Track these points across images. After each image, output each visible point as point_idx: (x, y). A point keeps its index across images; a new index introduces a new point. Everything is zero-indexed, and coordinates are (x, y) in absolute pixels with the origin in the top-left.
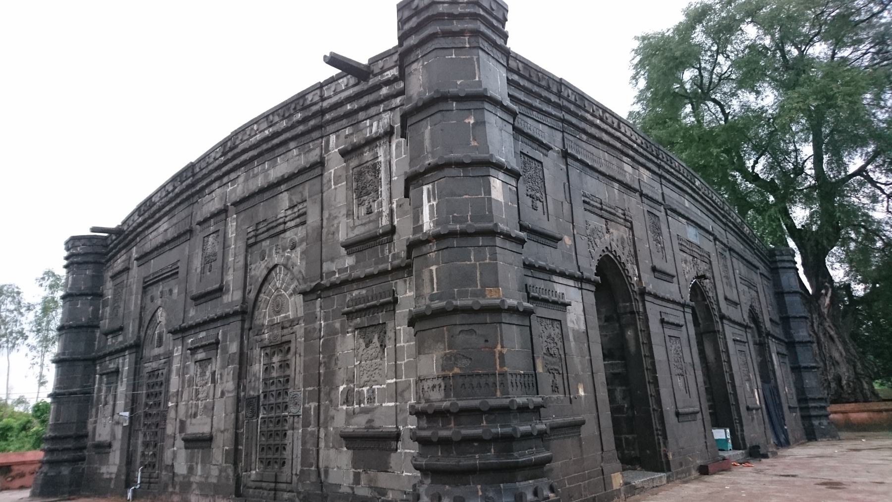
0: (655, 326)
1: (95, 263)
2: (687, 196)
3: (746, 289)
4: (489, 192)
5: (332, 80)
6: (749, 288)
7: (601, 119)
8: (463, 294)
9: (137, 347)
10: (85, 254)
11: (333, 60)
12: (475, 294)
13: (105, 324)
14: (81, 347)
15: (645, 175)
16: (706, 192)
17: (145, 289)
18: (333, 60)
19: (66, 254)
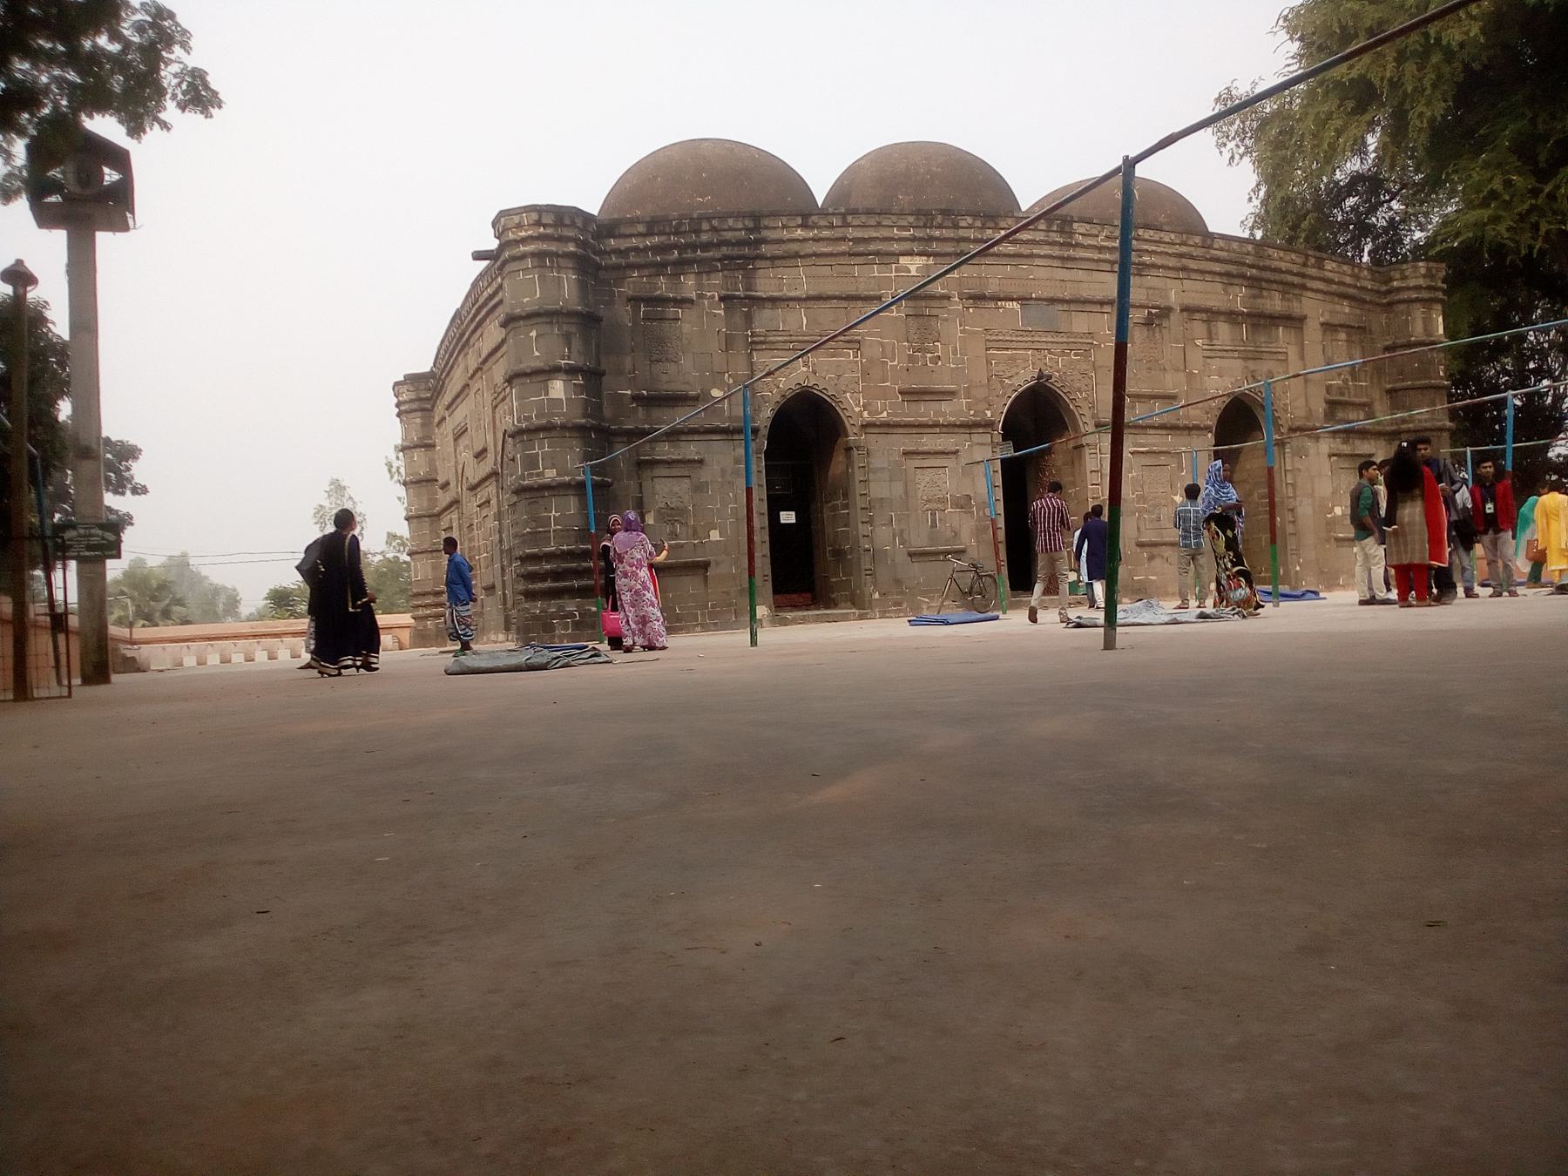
0: (877, 462)
1: (422, 410)
3: (1238, 364)
4: (547, 394)
5: (487, 269)
6: (1245, 359)
7: (804, 226)
8: (531, 475)
9: (455, 502)
10: (411, 401)
11: (478, 256)
12: (538, 475)
13: (441, 480)
14: (425, 504)
15: (914, 265)
17: (457, 438)
18: (478, 256)
19: (395, 400)
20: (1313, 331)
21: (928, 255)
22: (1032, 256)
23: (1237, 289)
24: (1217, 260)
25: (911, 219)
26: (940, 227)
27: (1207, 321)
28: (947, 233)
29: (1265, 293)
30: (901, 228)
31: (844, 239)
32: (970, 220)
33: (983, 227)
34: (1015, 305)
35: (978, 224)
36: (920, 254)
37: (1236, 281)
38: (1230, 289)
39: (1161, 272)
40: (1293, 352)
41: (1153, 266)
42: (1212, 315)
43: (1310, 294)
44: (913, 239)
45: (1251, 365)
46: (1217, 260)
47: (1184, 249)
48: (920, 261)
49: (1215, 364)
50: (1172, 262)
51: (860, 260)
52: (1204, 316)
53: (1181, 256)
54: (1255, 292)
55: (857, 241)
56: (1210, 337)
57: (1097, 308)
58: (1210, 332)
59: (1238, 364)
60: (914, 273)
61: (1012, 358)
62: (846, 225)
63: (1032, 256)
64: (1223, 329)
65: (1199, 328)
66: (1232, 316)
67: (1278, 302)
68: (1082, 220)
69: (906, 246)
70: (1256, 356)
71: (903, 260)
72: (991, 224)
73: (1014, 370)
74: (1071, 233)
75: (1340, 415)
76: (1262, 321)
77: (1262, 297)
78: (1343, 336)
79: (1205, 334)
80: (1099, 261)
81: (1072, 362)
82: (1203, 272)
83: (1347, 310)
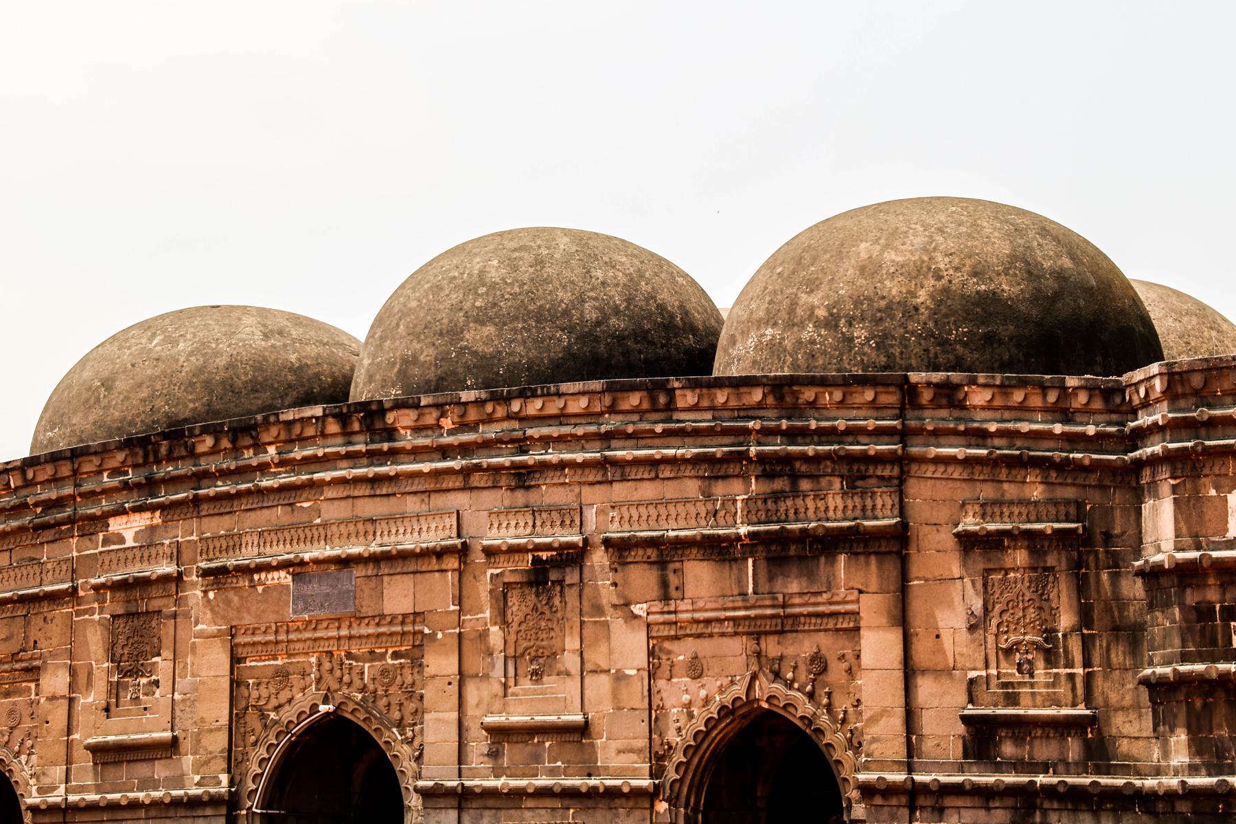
2: (330, 493)
6: (757, 636)
15: (129, 528)
16: (473, 415)
20: (936, 555)
21: (152, 508)
22: (314, 486)
23: (736, 486)
24: (682, 433)
25: (120, 456)
26: (170, 458)
27: (662, 564)
28: (185, 468)
29: (805, 485)
30: (115, 472)
31: (22, 507)
32: (209, 441)
33: (236, 451)
34: (284, 578)
35: (225, 443)
36: (138, 509)
37: (733, 469)
38: (720, 489)
39: (568, 476)
40: (873, 608)
41: (544, 466)
42: (665, 554)
43: (929, 470)
44: (126, 486)
45: (772, 647)
46: (682, 433)
47: (611, 423)
48: (141, 521)
49: (682, 652)
50: (591, 454)
51: (48, 535)
52: (652, 553)
53: (607, 437)
54: (779, 484)
55: (49, 505)
56: (665, 597)
57: (434, 563)
58: (664, 584)
59: (736, 649)
60: (130, 543)
61: (282, 675)
62: (28, 484)
63: (311, 485)
64: (700, 579)
65: (642, 578)
66: (718, 549)
67: (835, 501)
68: (399, 405)
69: (119, 499)
70: (786, 625)
71: (115, 525)
72: (248, 441)
73: (284, 696)
74: (390, 433)
75: (1008, 749)
76: (785, 551)
77: (796, 493)
78: (1020, 557)
79: (655, 592)
80: (437, 474)
81: (384, 672)
82: (652, 463)
83: (1037, 492)
